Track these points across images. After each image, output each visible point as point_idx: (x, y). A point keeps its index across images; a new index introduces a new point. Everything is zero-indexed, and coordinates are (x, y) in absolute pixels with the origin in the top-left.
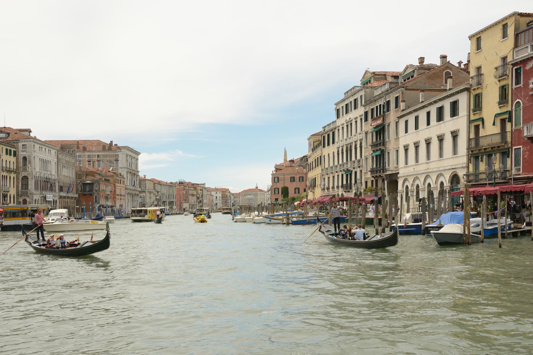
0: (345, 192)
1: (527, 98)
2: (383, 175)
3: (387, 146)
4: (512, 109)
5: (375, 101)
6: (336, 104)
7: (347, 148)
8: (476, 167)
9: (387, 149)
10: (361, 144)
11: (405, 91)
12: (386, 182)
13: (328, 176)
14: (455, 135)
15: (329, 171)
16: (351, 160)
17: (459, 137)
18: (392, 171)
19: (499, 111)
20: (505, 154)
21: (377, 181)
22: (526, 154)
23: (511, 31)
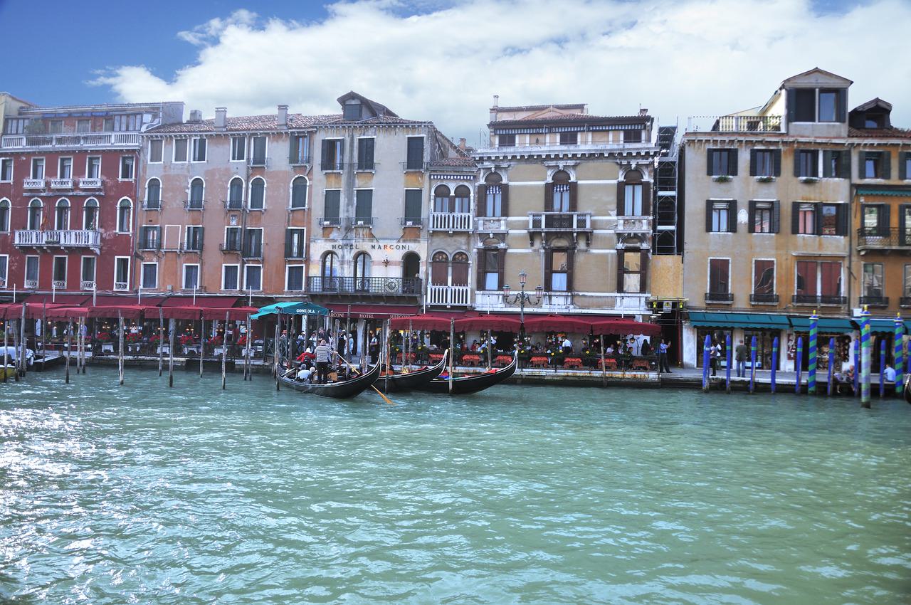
1: (19, 199)
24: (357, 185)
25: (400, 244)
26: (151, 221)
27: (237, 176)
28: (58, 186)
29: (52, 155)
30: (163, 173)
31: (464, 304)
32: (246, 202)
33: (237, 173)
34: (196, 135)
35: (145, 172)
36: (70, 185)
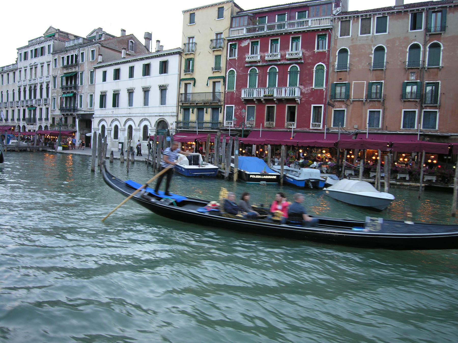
0: (28, 124)
1: (241, 69)
2: (75, 114)
3: (80, 90)
4: (226, 76)
5: (67, 51)
6: (18, 49)
7: (30, 87)
8: (186, 116)
9: (79, 93)
10: (48, 85)
11: (101, 47)
12: (77, 120)
13: (7, 109)
14: (163, 89)
15: (9, 105)
16: (35, 97)
17: (167, 91)
18: (85, 111)
19: (212, 75)
20: (216, 109)
21: (66, 119)
22: (238, 112)
23: (227, 14)
26: (340, 79)
27: (416, 43)
28: (271, 58)
29: (264, 38)
30: (351, 44)
32: (424, 61)
33: (415, 40)
35: (336, 44)
36: (279, 57)
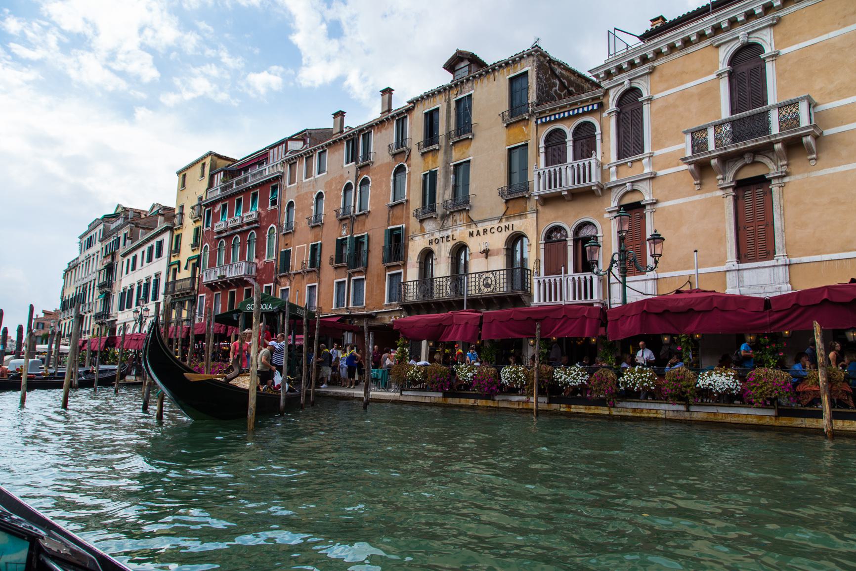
24: (453, 159)
25: (502, 225)
31: (589, 300)
33: (348, 178)
34: (319, 148)
